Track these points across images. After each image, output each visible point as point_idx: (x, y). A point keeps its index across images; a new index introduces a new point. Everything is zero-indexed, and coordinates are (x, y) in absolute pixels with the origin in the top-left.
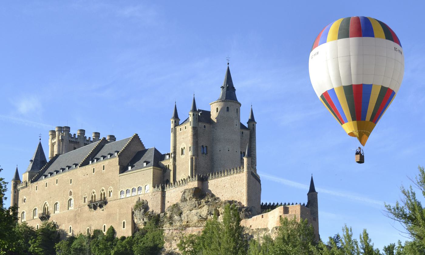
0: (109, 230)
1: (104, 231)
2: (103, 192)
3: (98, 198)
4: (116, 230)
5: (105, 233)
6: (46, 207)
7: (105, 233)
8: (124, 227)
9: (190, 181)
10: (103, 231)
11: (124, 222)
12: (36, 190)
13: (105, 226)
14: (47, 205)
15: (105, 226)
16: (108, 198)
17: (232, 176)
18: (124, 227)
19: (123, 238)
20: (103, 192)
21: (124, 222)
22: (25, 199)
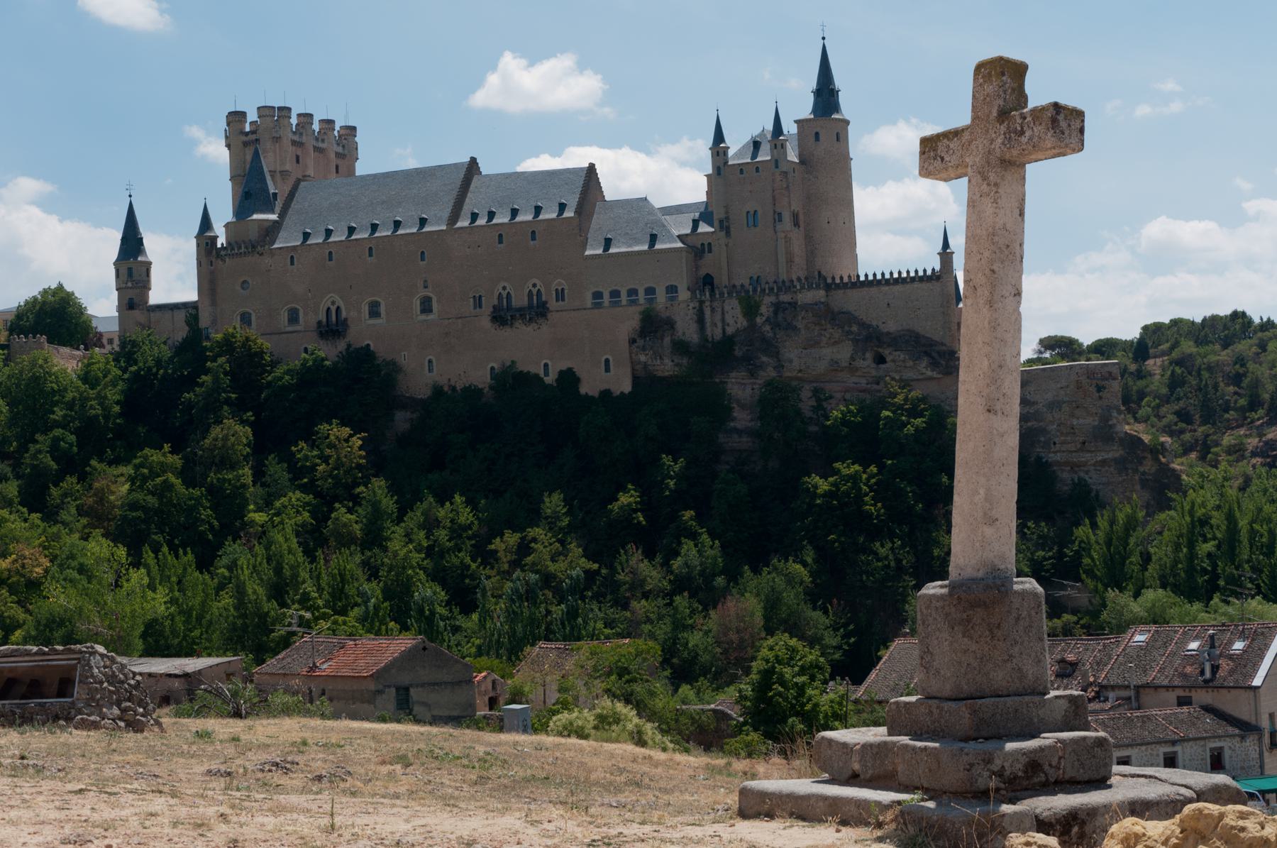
0: (561, 372)
1: (547, 374)
2: (535, 291)
3: (520, 300)
4: (580, 372)
5: (550, 379)
6: (333, 309)
7: (550, 379)
8: (607, 370)
9: (802, 288)
10: (542, 374)
11: (607, 361)
12: (292, 263)
13: (546, 365)
14: (333, 303)
15: (546, 365)
16: (553, 304)
17: (908, 286)
18: (607, 370)
19: (606, 394)
20: (535, 291)
21: (607, 361)
22: (245, 282)
